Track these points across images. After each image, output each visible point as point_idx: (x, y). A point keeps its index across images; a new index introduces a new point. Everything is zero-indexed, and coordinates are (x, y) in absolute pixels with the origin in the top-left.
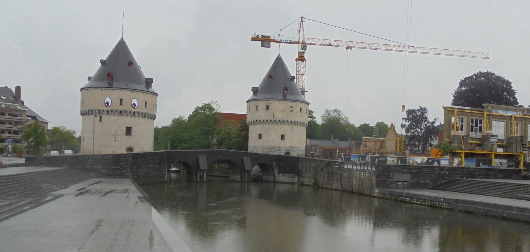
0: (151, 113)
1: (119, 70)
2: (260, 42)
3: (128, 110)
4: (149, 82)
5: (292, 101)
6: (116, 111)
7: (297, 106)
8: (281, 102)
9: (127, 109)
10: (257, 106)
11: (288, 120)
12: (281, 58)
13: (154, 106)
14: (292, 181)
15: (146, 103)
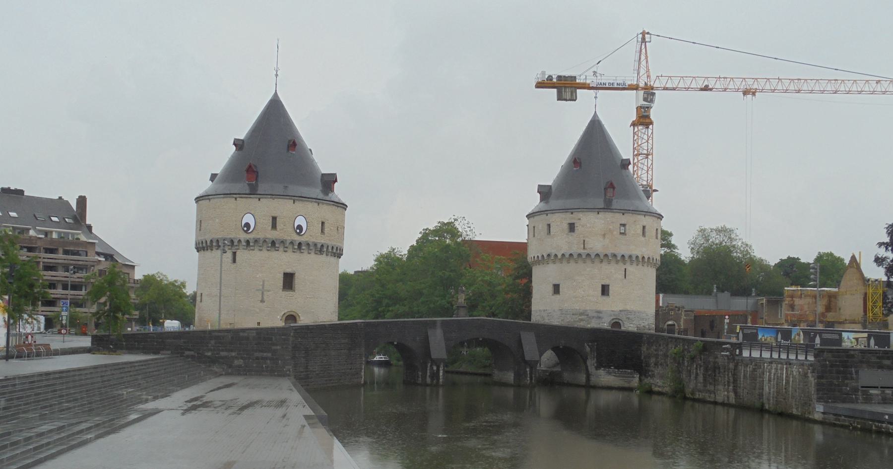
0: (334, 243)
1: (270, 158)
2: (555, 90)
3: (289, 238)
4: (329, 182)
5: (624, 212)
6: (265, 241)
7: (635, 223)
8: (601, 215)
9: (286, 238)
10: (549, 225)
11: (616, 252)
12: (599, 122)
13: (340, 229)
14: (626, 385)
15: (323, 223)
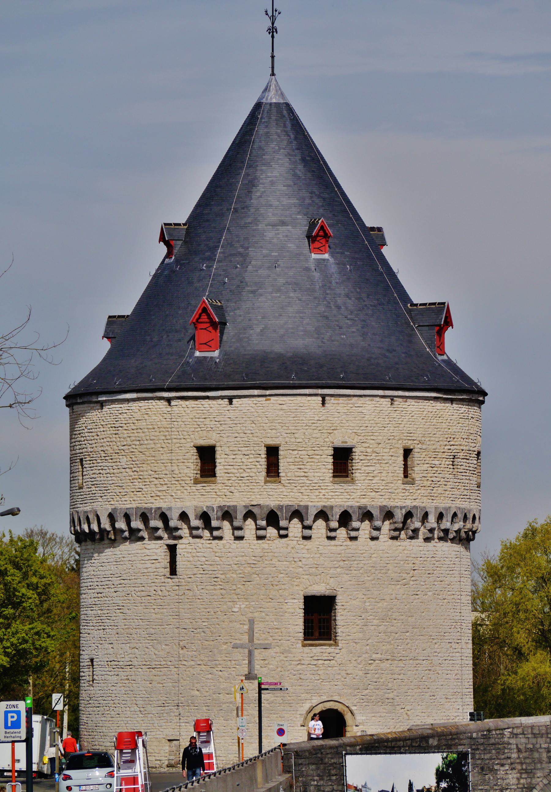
3: (313, 502)
6: (249, 514)
